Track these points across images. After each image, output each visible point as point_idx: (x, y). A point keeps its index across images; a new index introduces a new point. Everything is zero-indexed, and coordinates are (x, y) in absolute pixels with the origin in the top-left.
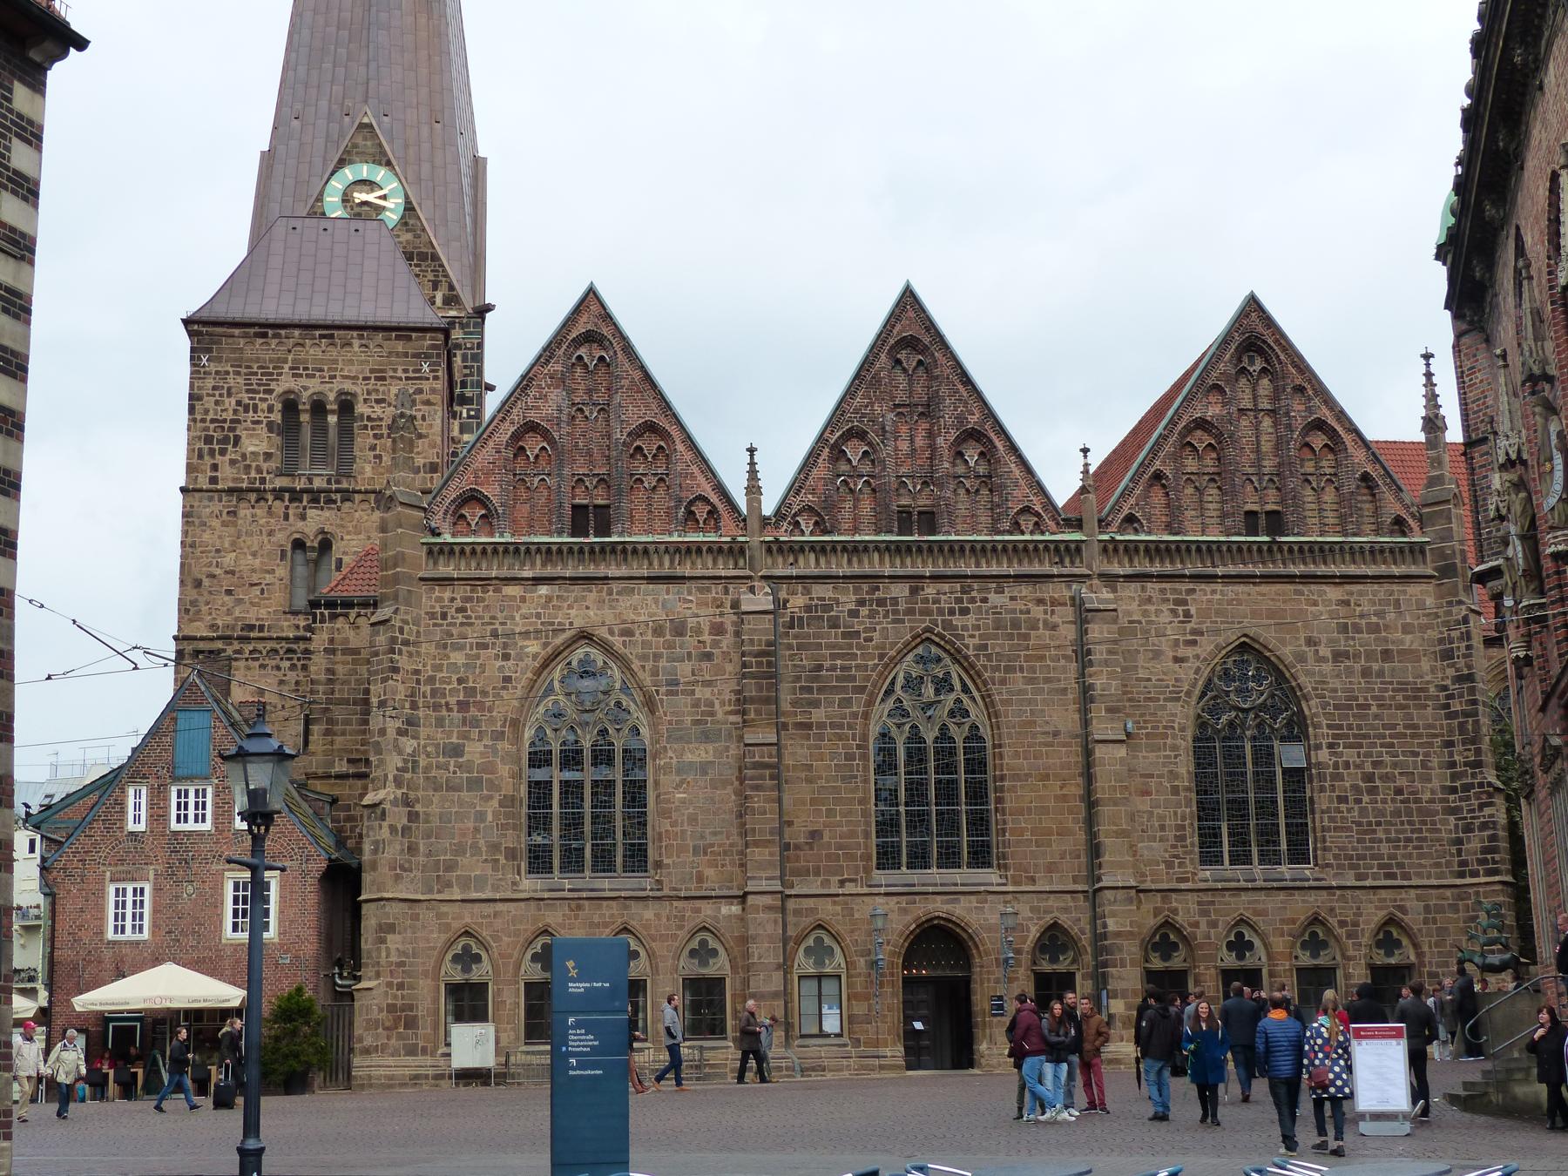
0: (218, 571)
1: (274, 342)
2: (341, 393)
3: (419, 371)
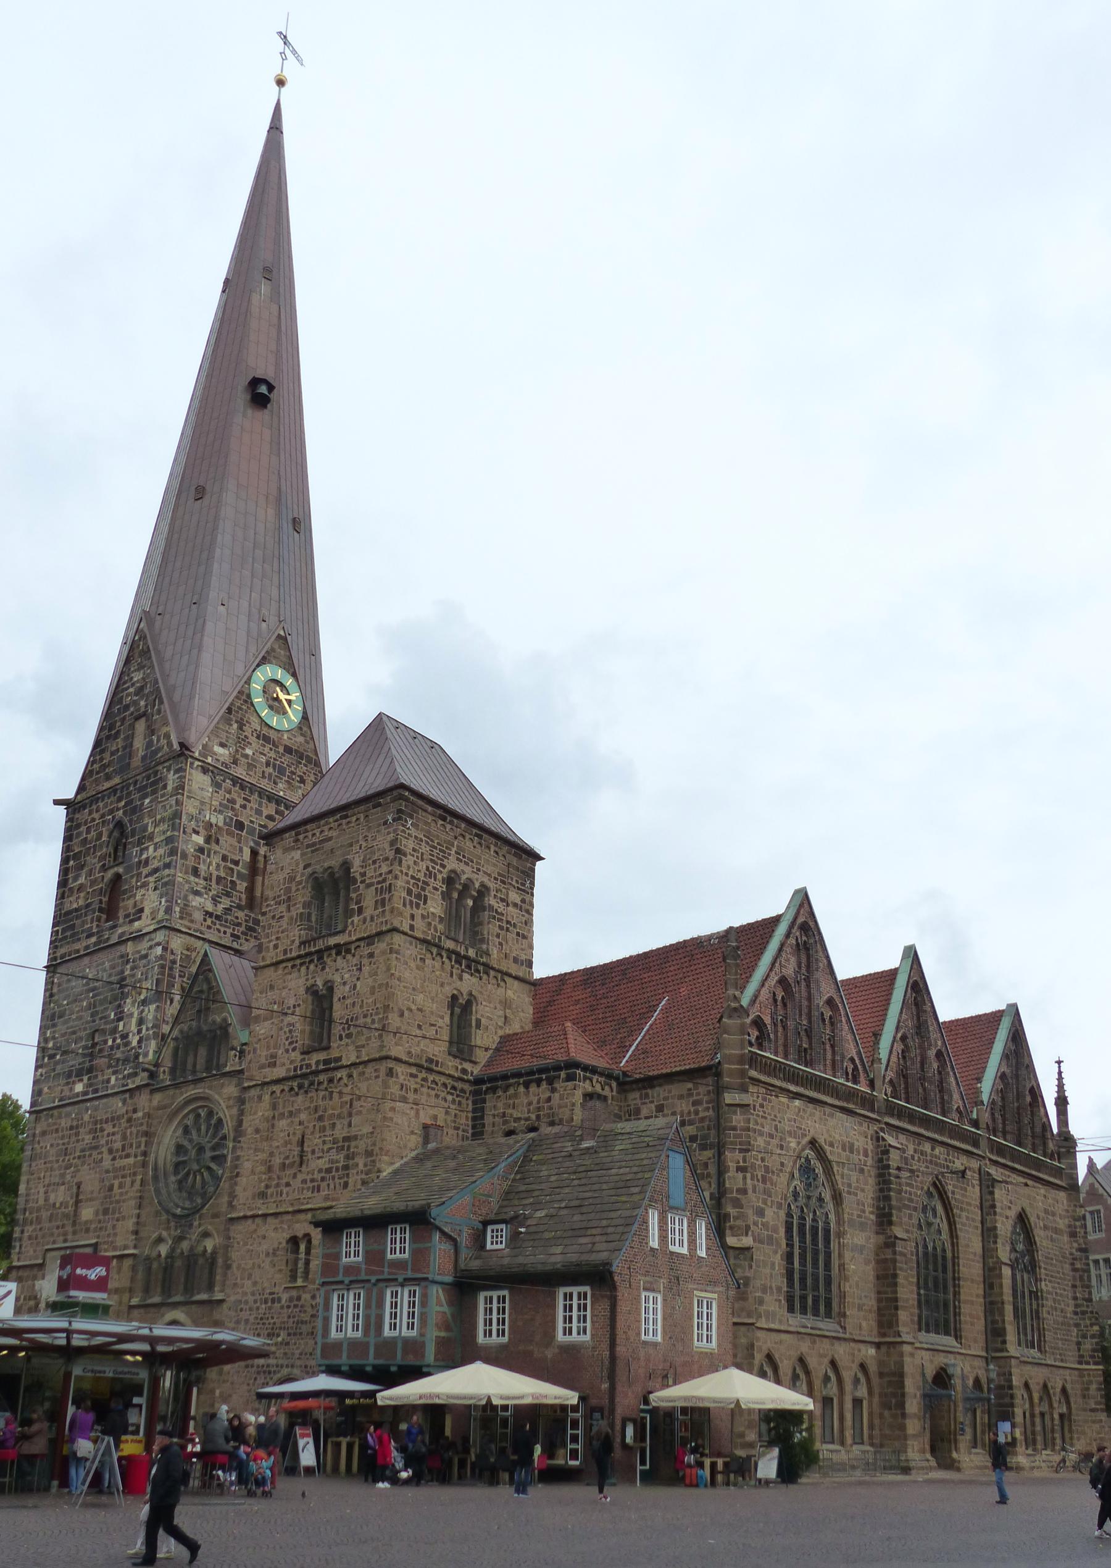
0: (414, 1007)
1: (449, 827)
2: (483, 885)
3: (523, 885)
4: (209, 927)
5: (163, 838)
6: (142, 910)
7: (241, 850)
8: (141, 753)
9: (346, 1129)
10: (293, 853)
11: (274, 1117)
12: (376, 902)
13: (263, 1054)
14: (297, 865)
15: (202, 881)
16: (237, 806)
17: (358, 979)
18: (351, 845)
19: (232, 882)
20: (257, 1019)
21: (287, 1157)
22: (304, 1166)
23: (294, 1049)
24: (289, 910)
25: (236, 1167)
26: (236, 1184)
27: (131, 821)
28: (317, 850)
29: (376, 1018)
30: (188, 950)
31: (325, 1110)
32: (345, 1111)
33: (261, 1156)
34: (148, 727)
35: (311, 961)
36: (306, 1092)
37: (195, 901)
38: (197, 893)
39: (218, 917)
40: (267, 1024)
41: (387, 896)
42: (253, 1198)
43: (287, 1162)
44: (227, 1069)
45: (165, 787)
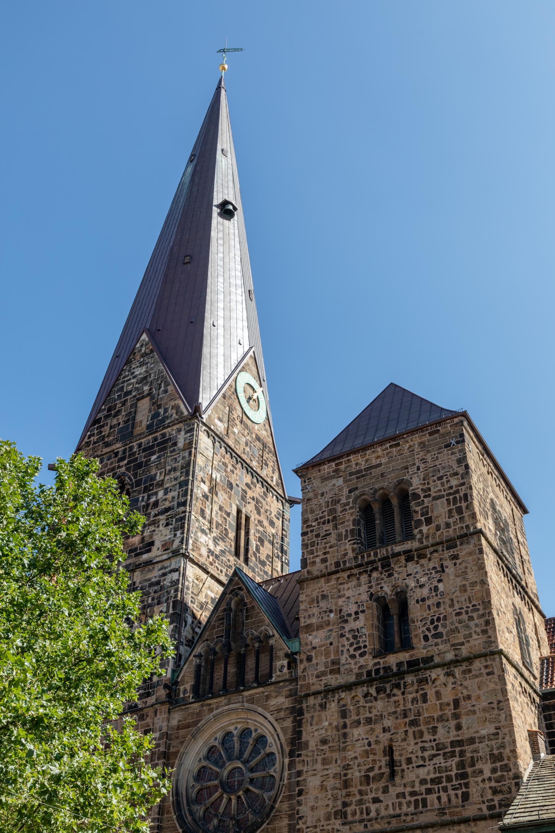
4: (211, 564)
5: (174, 483)
6: (152, 544)
7: (231, 506)
8: (145, 423)
9: (453, 732)
10: (334, 481)
11: (345, 726)
12: (450, 511)
13: (320, 662)
14: (341, 489)
15: (207, 523)
16: (229, 470)
17: (440, 581)
18: (406, 468)
19: (226, 529)
20: (309, 628)
21: (372, 769)
22: (397, 779)
23: (362, 655)
24: (335, 527)
25: (298, 784)
26: (299, 803)
27: (135, 475)
28: (363, 476)
29: (475, 615)
30: (197, 579)
31: (419, 714)
32: (449, 711)
33: (333, 769)
34: (153, 404)
35: (376, 569)
36: (389, 696)
37: (203, 539)
38: (203, 531)
39: (217, 557)
40: (322, 633)
41: (464, 505)
42: (328, 818)
43: (371, 774)
44: (273, 680)
45: (175, 444)
